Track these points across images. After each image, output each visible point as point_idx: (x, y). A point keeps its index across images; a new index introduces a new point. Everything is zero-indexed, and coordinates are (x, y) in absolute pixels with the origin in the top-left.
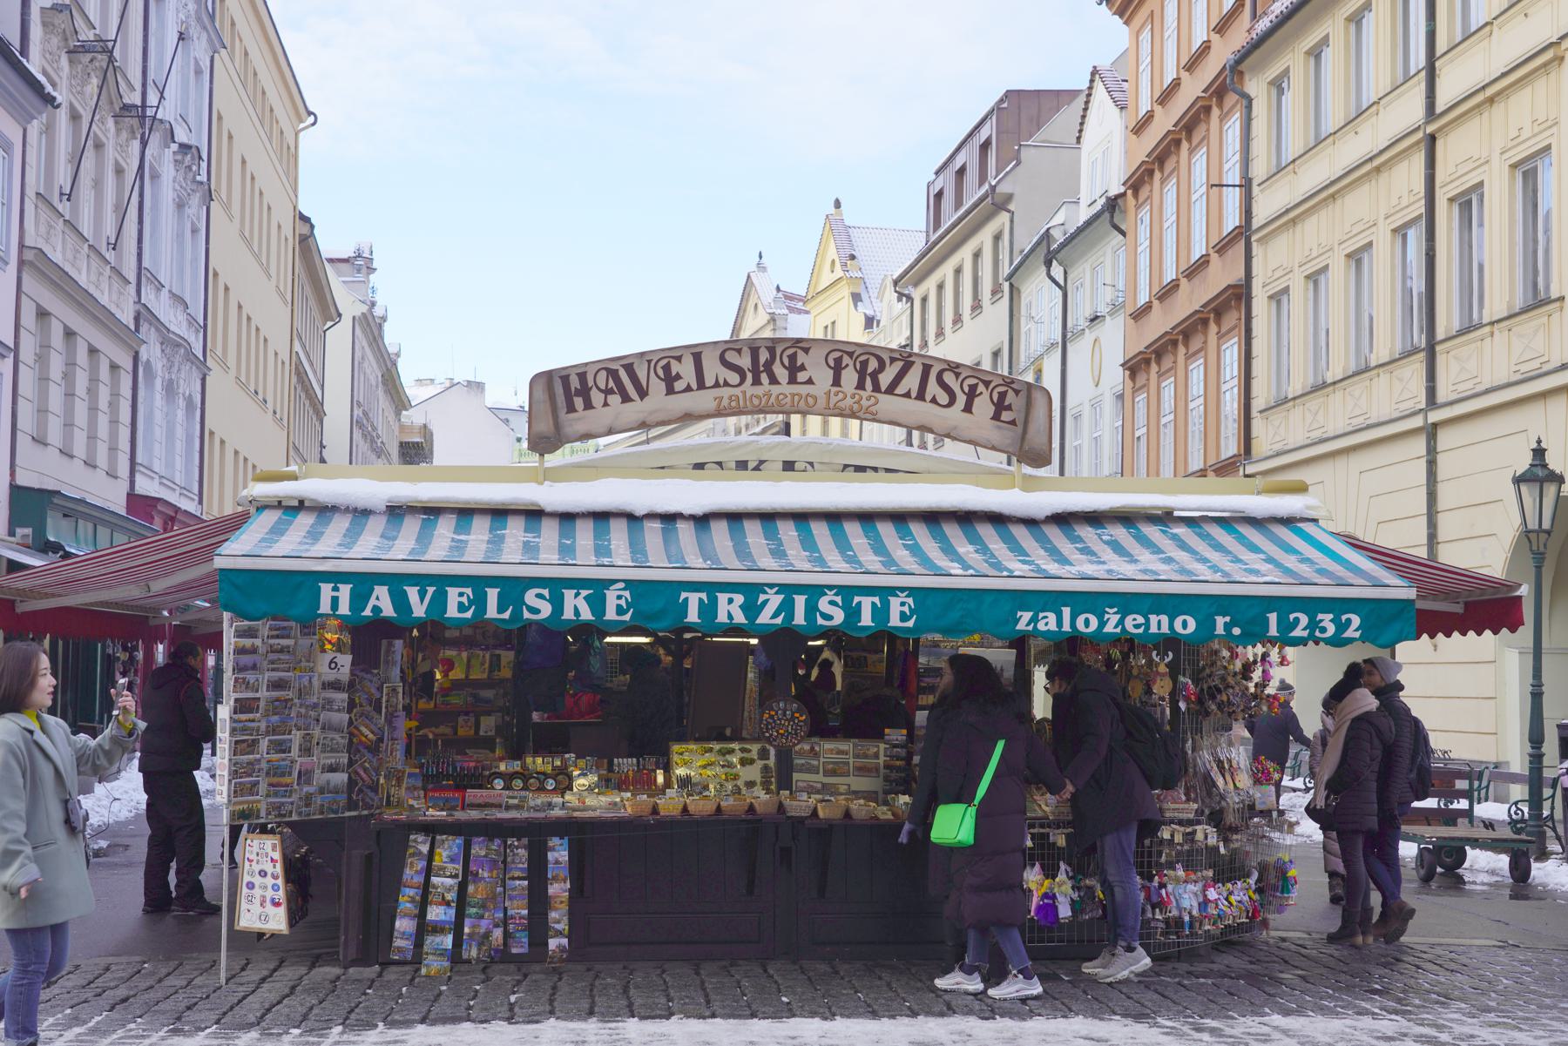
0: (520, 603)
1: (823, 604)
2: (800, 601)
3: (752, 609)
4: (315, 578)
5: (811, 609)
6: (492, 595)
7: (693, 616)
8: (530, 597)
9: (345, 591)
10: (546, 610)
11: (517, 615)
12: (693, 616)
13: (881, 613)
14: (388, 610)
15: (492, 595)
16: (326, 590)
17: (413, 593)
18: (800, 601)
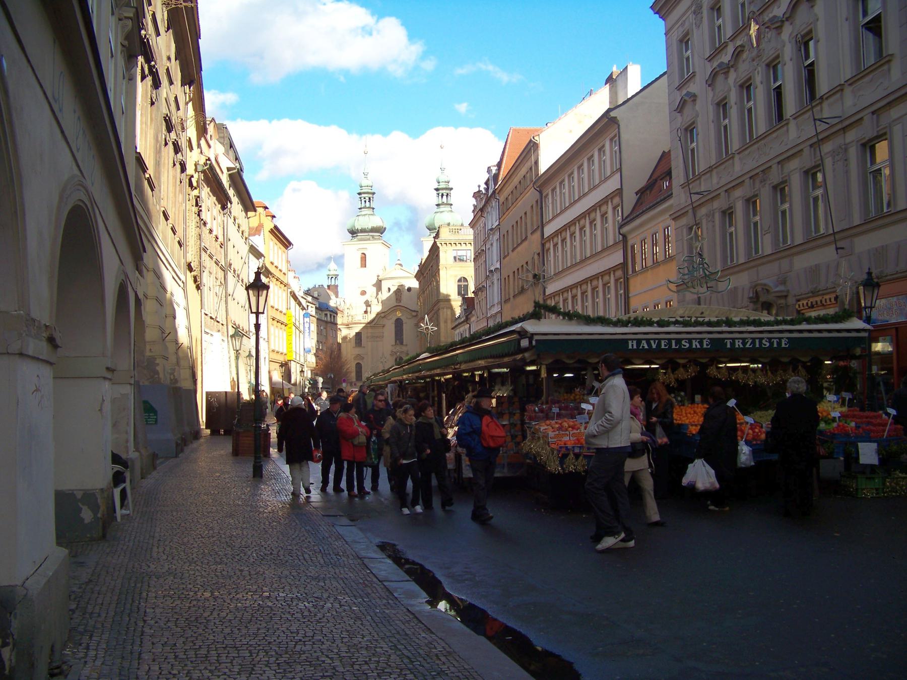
0: (681, 344)
1: (764, 341)
2: (757, 341)
3: (744, 343)
4: (626, 341)
5: (760, 343)
6: (673, 342)
7: (729, 346)
8: (683, 342)
9: (635, 342)
10: (688, 345)
11: (680, 346)
12: (729, 346)
13: (779, 344)
14: (646, 347)
15: (673, 342)
16: (630, 342)
17: (652, 342)
18: (757, 341)
